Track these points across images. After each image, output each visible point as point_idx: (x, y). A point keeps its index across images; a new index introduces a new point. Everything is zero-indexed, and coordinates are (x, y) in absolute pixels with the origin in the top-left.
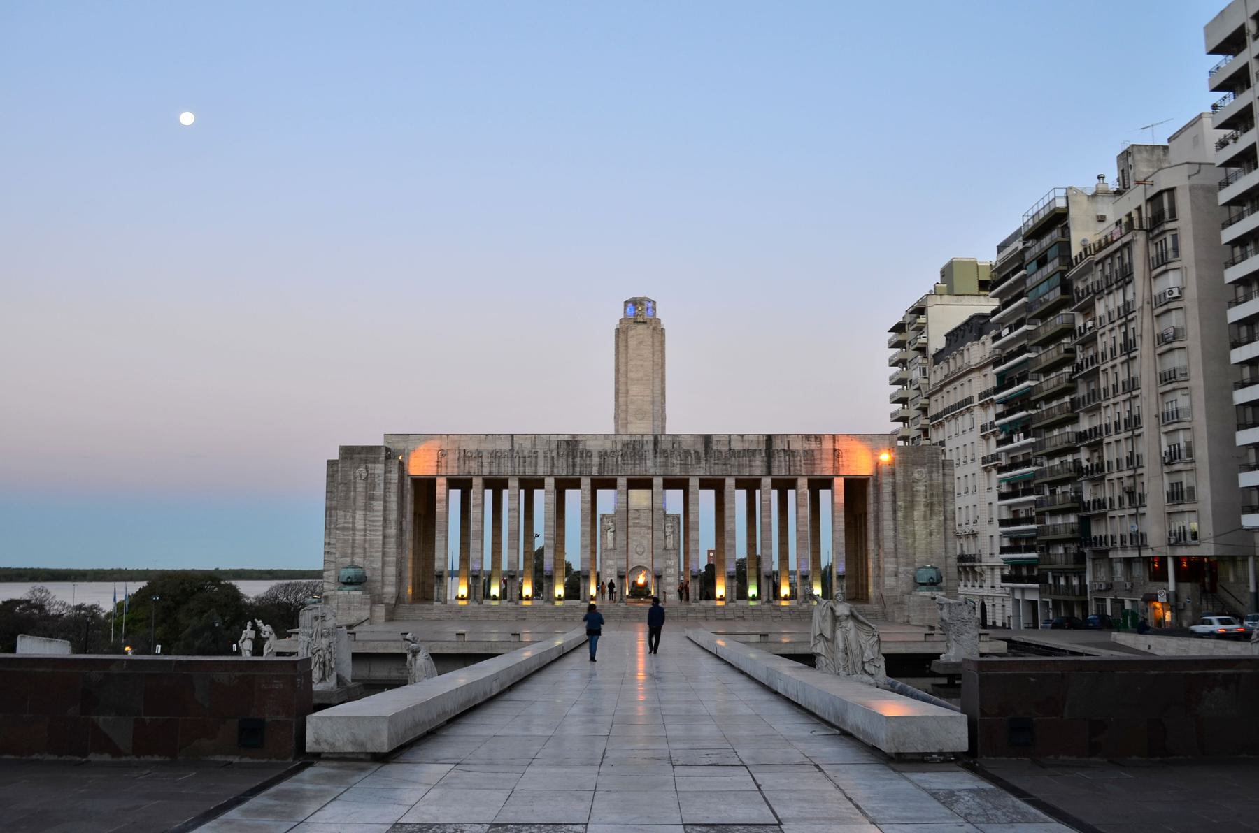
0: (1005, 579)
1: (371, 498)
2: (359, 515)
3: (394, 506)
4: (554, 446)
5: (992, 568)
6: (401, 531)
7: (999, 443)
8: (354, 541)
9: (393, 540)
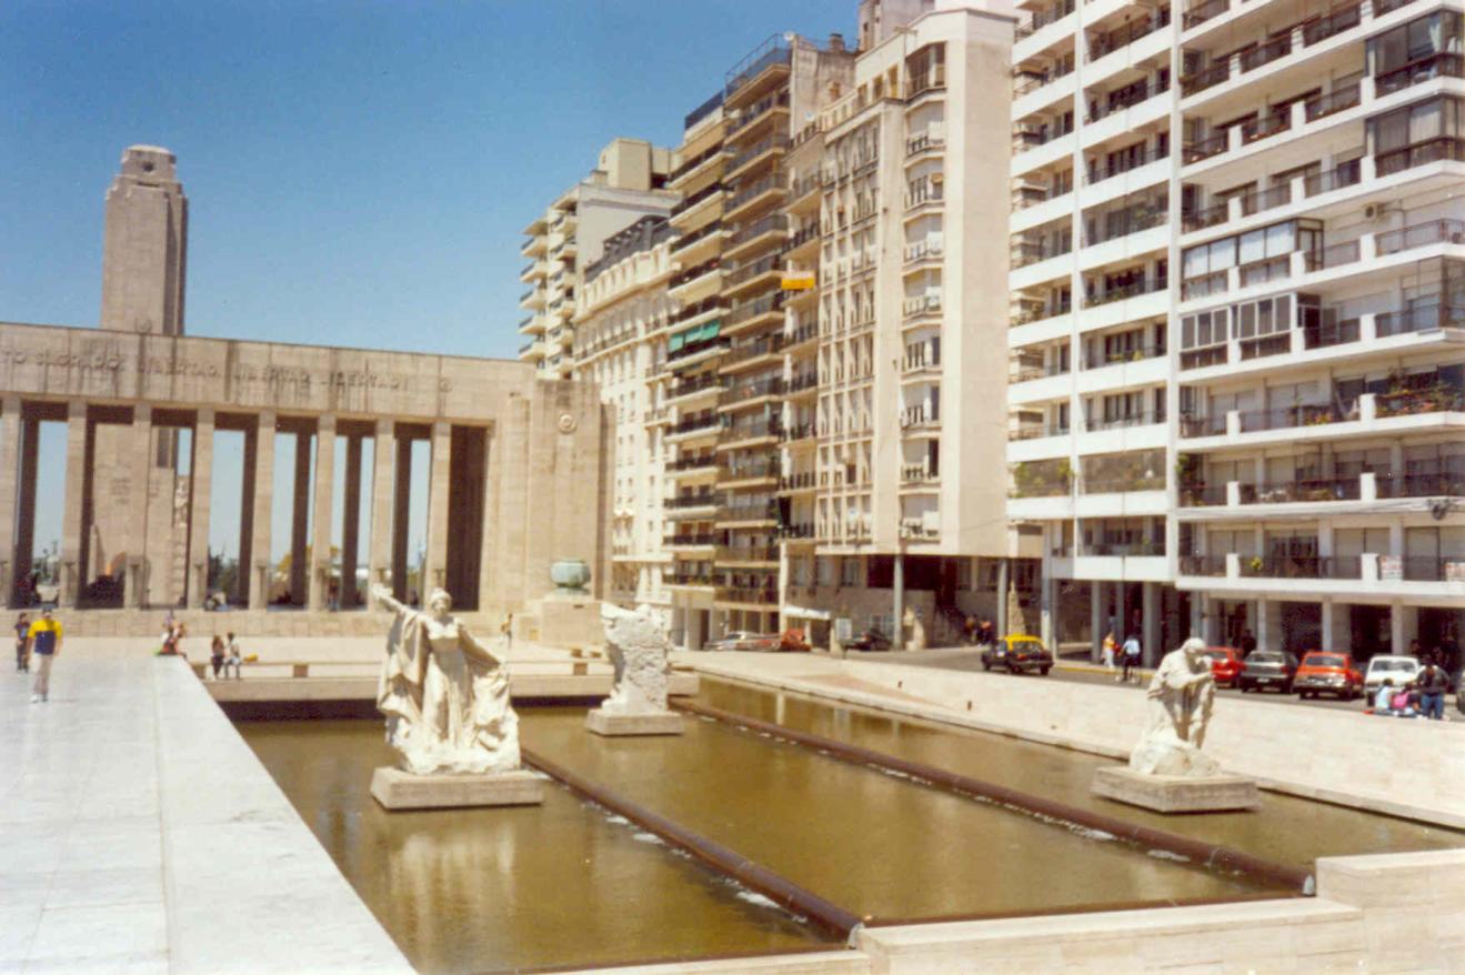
0: (666, 579)
5: (649, 565)
7: (669, 394)
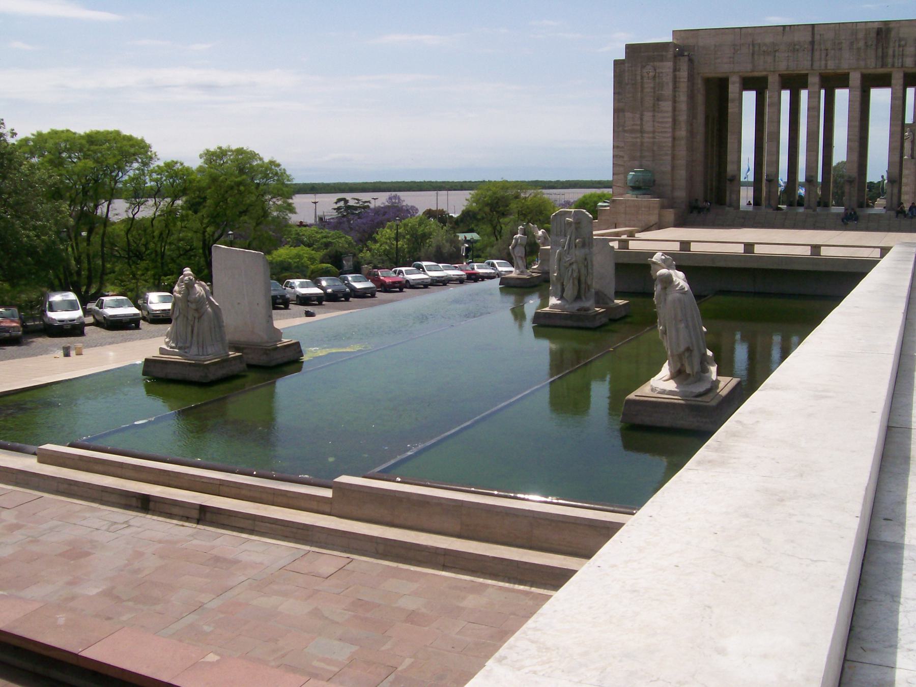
1: (659, 99)
2: (648, 116)
3: (683, 106)
4: (861, 35)
6: (692, 133)
8: (642, 143)
9: (683, 142)
